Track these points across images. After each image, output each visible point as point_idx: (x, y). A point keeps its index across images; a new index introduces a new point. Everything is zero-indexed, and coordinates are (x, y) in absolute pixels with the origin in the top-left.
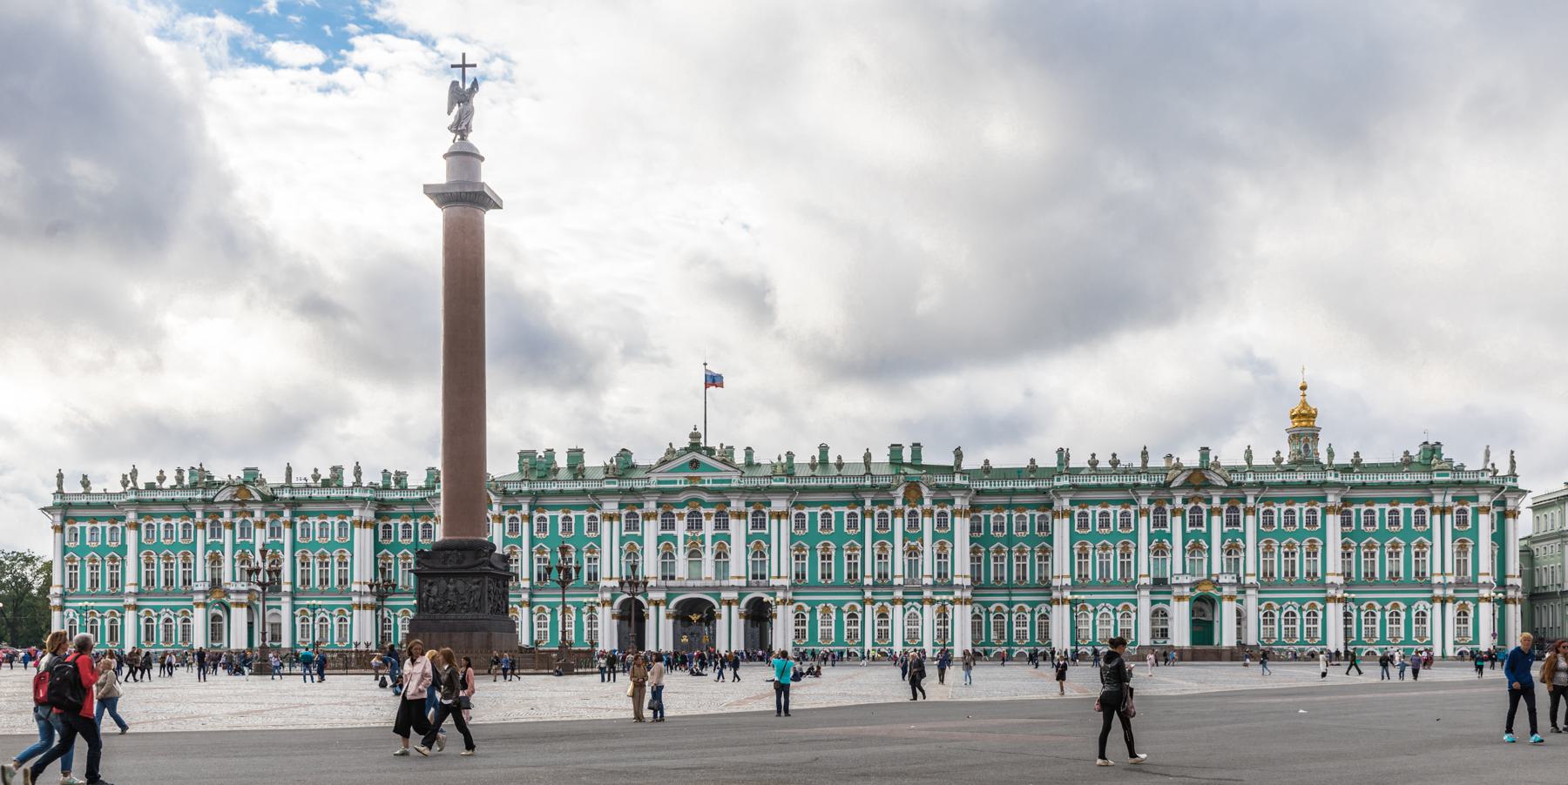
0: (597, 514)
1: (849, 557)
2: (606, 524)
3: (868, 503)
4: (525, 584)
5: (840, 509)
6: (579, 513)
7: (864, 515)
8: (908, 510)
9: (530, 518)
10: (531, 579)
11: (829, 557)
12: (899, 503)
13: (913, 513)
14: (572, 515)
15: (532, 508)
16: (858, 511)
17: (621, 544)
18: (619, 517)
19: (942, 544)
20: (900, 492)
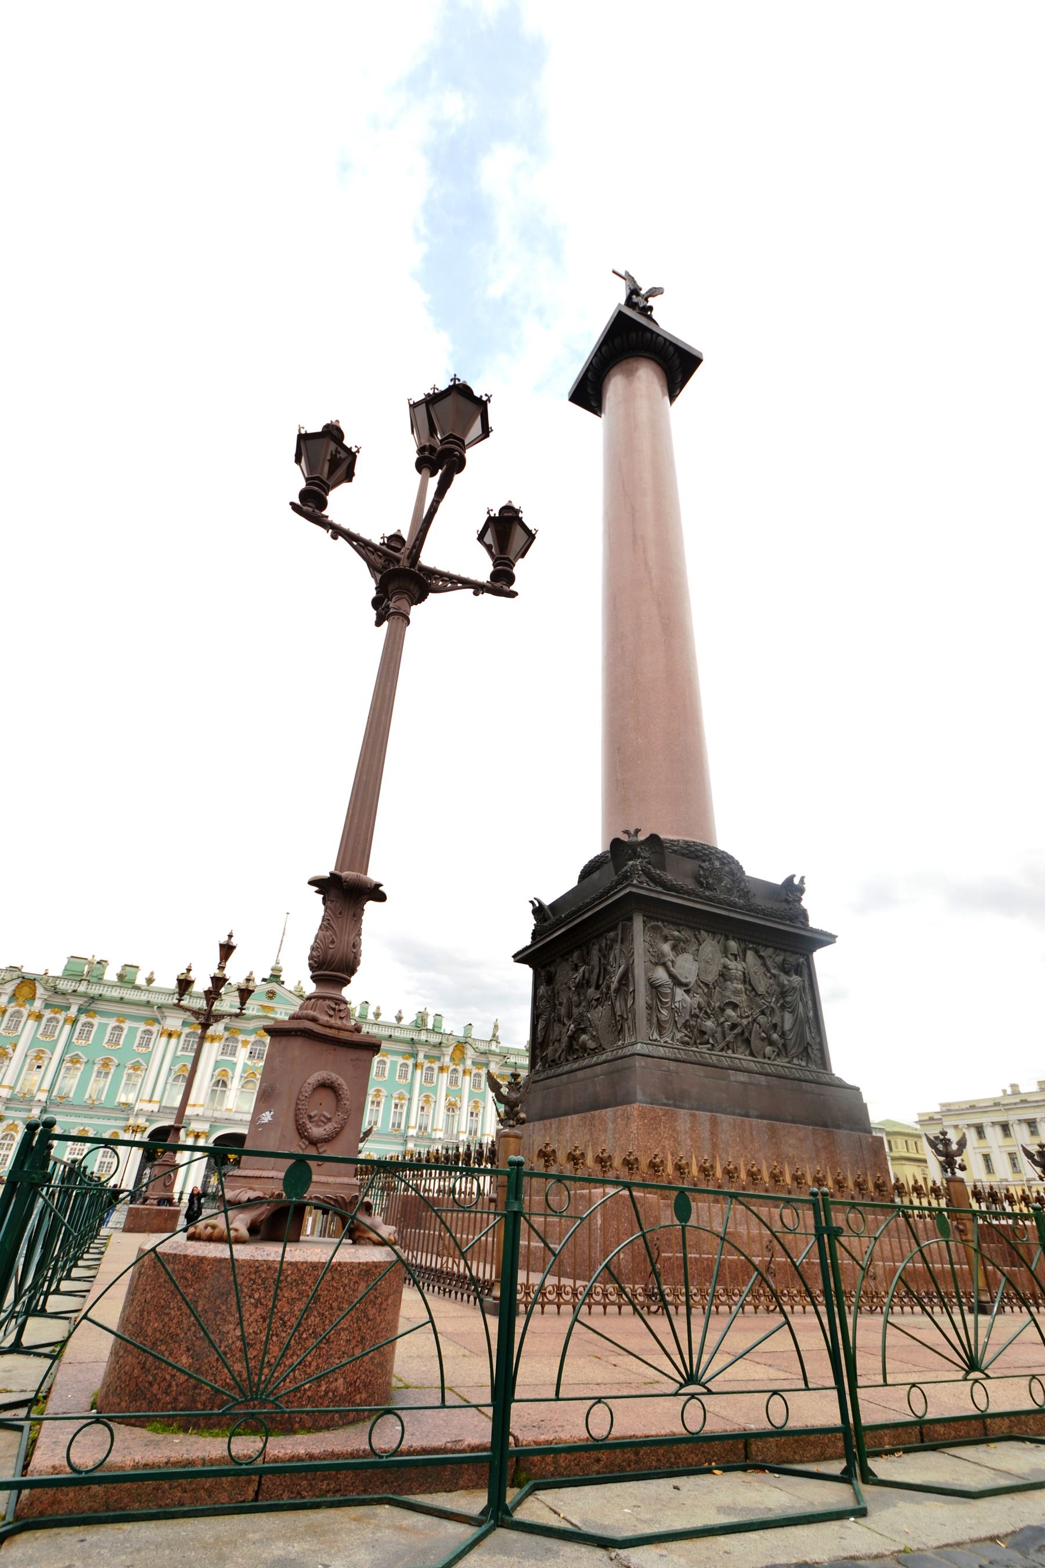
0: (155, 1028)
1: (396, 1106)
2: (164, 1039)
3: (421, 1056)
4: (42, 1096)
5: (395, 1058)
6: (134, 1025)
7: (416, 1066)
8: (452, 1067)
9: (75, 1022)
10: (50, 1091)
11: (378, 1103)
12: (447, 1059)
13: (455, 1070)
14: (126, 1026)
15: (80, 1011)
16: (410, 1062)
17: (173, 1064)
18: (179, 1036)
19: (476, 1102)
20: (451, 1049)
